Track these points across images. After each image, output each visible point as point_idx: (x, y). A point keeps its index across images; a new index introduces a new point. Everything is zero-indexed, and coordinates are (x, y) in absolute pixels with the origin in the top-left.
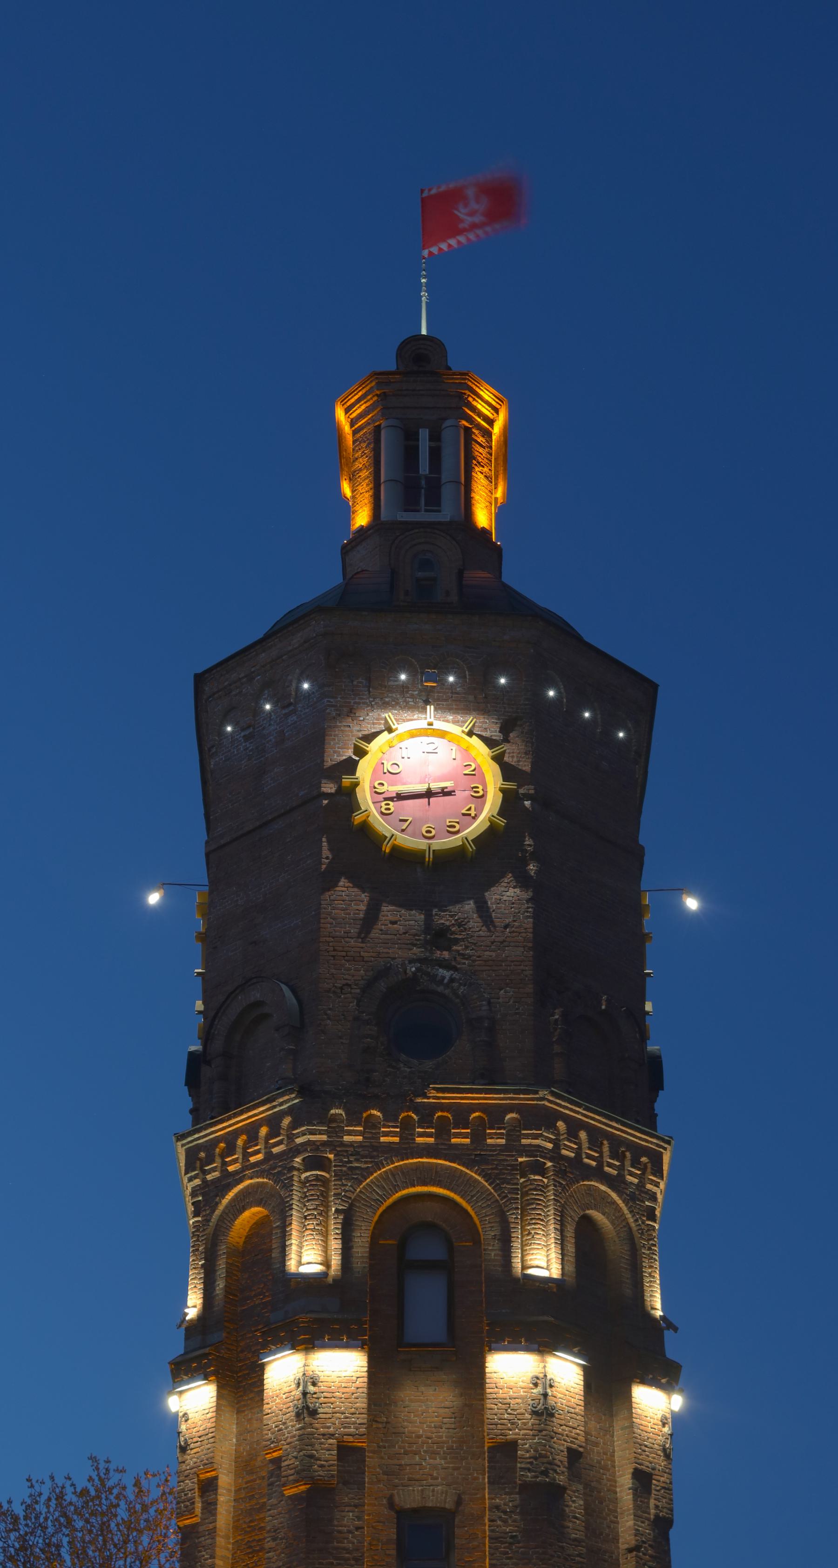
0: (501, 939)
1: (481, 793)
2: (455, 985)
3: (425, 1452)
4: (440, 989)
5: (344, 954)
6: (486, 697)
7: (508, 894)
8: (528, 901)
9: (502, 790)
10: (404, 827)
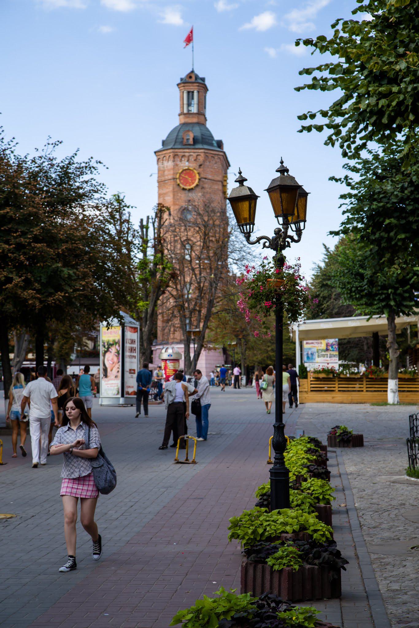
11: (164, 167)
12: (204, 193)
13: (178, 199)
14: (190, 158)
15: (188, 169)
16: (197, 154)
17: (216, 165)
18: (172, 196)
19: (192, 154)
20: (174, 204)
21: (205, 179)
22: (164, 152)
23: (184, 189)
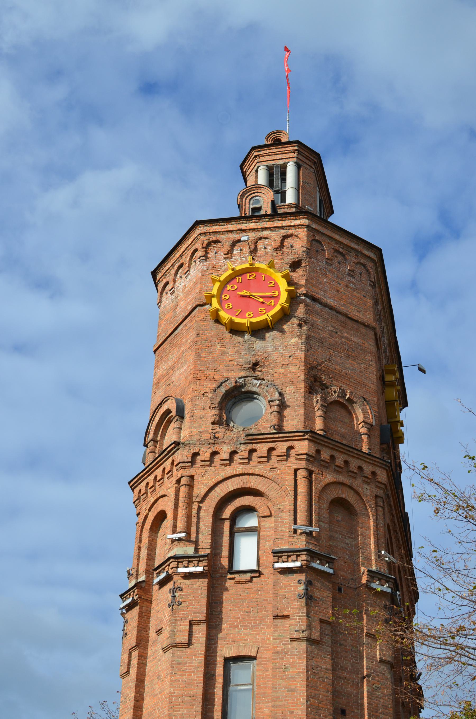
0: (288, 362)
1: (277, 294)
2: (263, 386)
3: (241, 626)
5: (205, 378)
6: (282, 253)
7: (292, 341)
8: (302, 343)
9: (287, 291)
10: (237, 314)
11: (177, 297)
12: (308, 337)
13: (213, 361)
14: (260, 246)
16: (282, 232)
17: (352, 280)
18: (191, 357)
20: (198, 376)
21: (314, 299)
22: (178, 254)
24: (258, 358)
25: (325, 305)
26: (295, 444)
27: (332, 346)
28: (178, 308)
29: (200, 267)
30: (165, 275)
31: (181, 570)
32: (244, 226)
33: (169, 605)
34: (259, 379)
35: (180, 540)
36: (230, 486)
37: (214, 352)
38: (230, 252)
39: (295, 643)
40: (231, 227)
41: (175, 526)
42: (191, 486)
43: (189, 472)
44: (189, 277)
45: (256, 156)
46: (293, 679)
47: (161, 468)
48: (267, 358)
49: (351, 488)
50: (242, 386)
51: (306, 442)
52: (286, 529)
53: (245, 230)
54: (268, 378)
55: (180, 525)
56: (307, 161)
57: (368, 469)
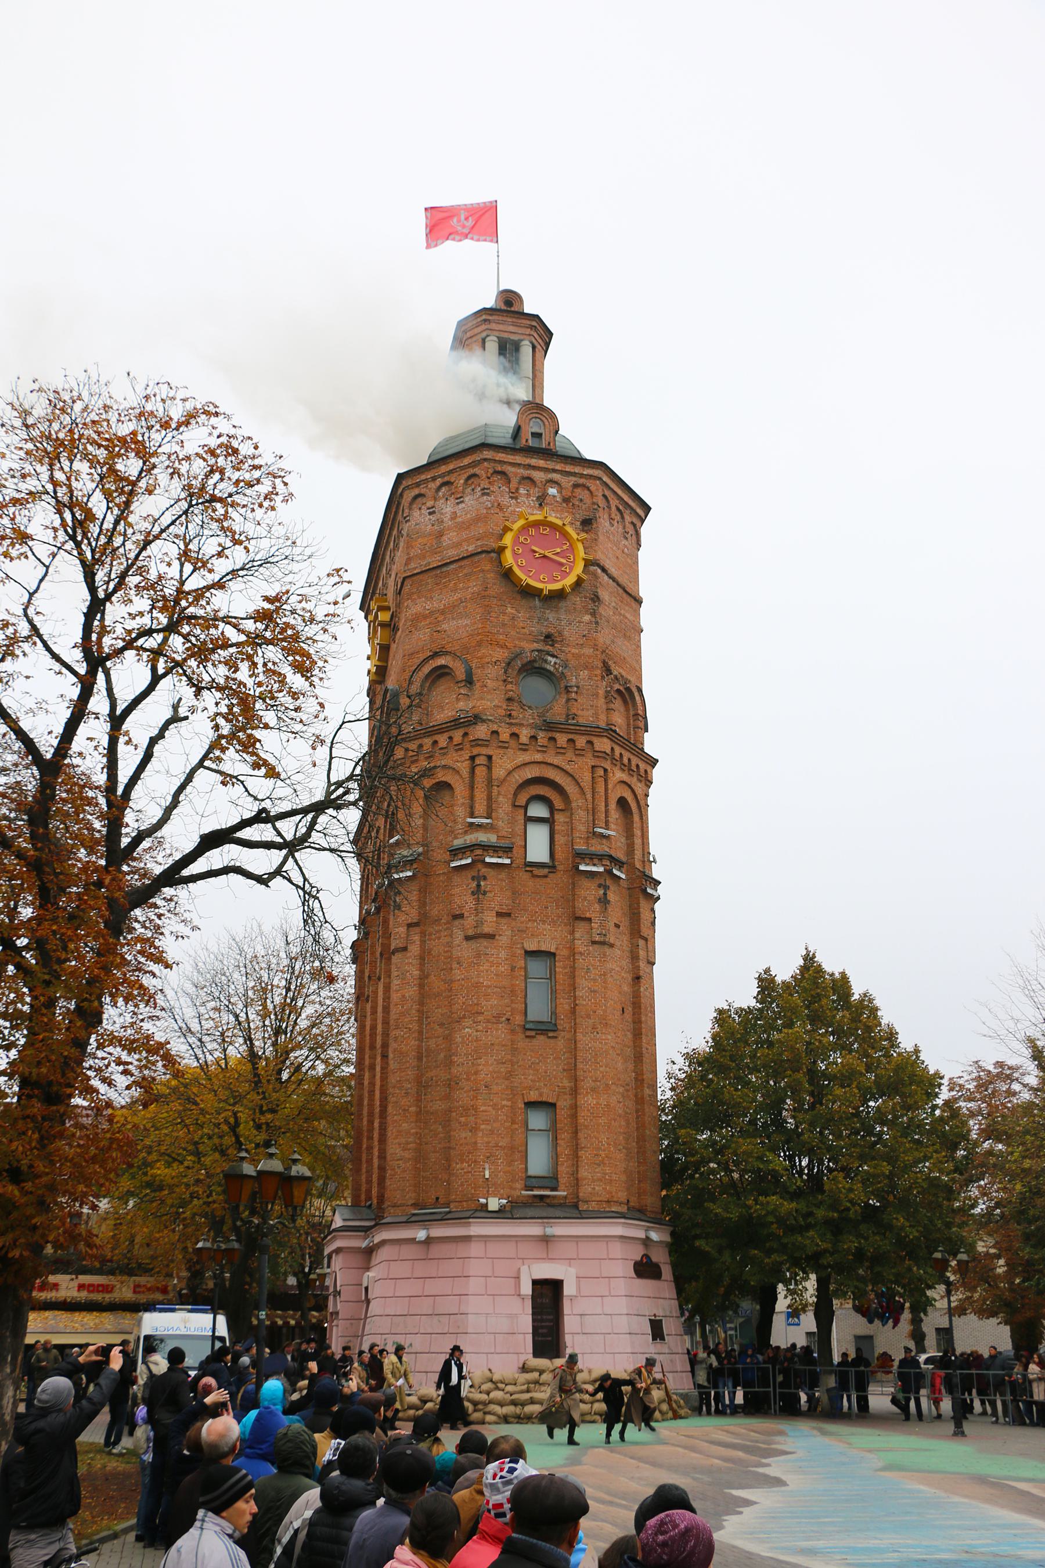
4: (548, 667)
13: (504, 625)
15: (544, 523)
19: (556, 476)
21: (604, 570)
22: (444, 469)
23: (528, 593)
24: (551, 630)
25: (611, 577)
26: (595, 740)
27: (614, 627)
28: (444, 538)
29: (481, 500)
30: (418, 485)
31: (488, 860)
32: (533, 462)
33: (473, 893)
34: (553, 656)
35: (480, 826)
36: (530, 773)
37: (504, 614)
38: (517, 489)
39: (596, 946)
40: (518, 459)
41: (472, 807)
42: (489, 768)
43: (484, 751)
44: (463, 505)
45: (485, 320)
46: (595, 980)
47: (446, 736)
48: (560, 633)
49: (630, 786)
50: (534, 661)
51: (605, 740)
52: (581, 828)
53: (534, 468)
54: (562, 656)
55: (480, 807)
56: (540, 341)
57: (643, 766)
